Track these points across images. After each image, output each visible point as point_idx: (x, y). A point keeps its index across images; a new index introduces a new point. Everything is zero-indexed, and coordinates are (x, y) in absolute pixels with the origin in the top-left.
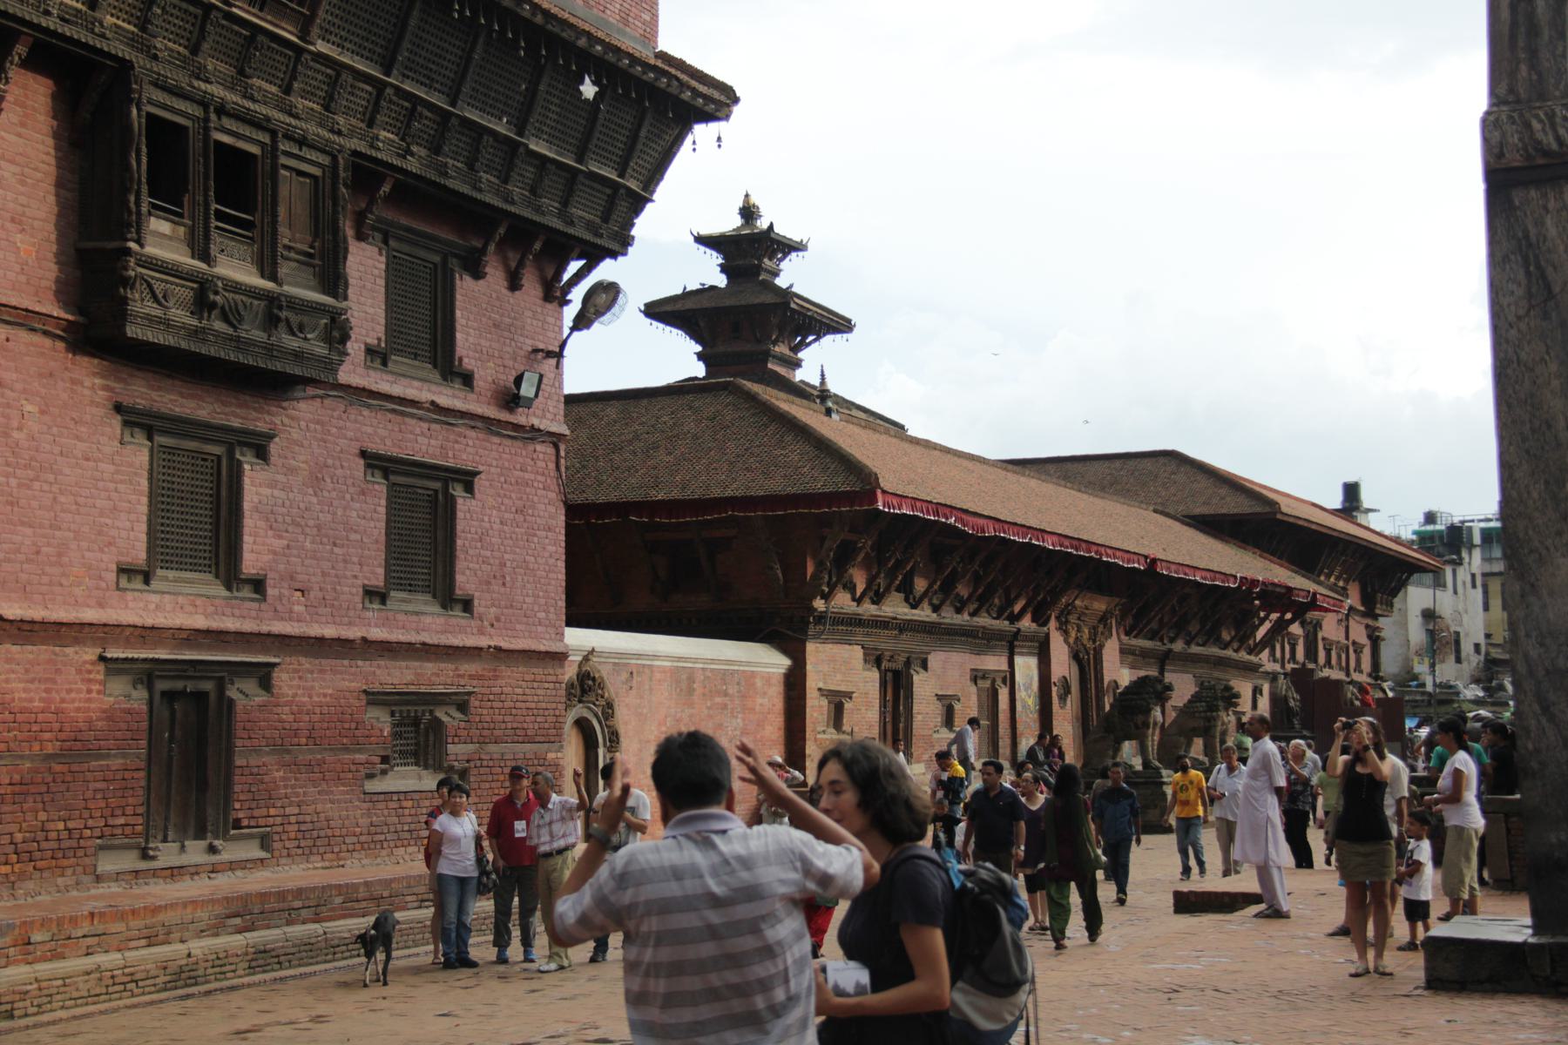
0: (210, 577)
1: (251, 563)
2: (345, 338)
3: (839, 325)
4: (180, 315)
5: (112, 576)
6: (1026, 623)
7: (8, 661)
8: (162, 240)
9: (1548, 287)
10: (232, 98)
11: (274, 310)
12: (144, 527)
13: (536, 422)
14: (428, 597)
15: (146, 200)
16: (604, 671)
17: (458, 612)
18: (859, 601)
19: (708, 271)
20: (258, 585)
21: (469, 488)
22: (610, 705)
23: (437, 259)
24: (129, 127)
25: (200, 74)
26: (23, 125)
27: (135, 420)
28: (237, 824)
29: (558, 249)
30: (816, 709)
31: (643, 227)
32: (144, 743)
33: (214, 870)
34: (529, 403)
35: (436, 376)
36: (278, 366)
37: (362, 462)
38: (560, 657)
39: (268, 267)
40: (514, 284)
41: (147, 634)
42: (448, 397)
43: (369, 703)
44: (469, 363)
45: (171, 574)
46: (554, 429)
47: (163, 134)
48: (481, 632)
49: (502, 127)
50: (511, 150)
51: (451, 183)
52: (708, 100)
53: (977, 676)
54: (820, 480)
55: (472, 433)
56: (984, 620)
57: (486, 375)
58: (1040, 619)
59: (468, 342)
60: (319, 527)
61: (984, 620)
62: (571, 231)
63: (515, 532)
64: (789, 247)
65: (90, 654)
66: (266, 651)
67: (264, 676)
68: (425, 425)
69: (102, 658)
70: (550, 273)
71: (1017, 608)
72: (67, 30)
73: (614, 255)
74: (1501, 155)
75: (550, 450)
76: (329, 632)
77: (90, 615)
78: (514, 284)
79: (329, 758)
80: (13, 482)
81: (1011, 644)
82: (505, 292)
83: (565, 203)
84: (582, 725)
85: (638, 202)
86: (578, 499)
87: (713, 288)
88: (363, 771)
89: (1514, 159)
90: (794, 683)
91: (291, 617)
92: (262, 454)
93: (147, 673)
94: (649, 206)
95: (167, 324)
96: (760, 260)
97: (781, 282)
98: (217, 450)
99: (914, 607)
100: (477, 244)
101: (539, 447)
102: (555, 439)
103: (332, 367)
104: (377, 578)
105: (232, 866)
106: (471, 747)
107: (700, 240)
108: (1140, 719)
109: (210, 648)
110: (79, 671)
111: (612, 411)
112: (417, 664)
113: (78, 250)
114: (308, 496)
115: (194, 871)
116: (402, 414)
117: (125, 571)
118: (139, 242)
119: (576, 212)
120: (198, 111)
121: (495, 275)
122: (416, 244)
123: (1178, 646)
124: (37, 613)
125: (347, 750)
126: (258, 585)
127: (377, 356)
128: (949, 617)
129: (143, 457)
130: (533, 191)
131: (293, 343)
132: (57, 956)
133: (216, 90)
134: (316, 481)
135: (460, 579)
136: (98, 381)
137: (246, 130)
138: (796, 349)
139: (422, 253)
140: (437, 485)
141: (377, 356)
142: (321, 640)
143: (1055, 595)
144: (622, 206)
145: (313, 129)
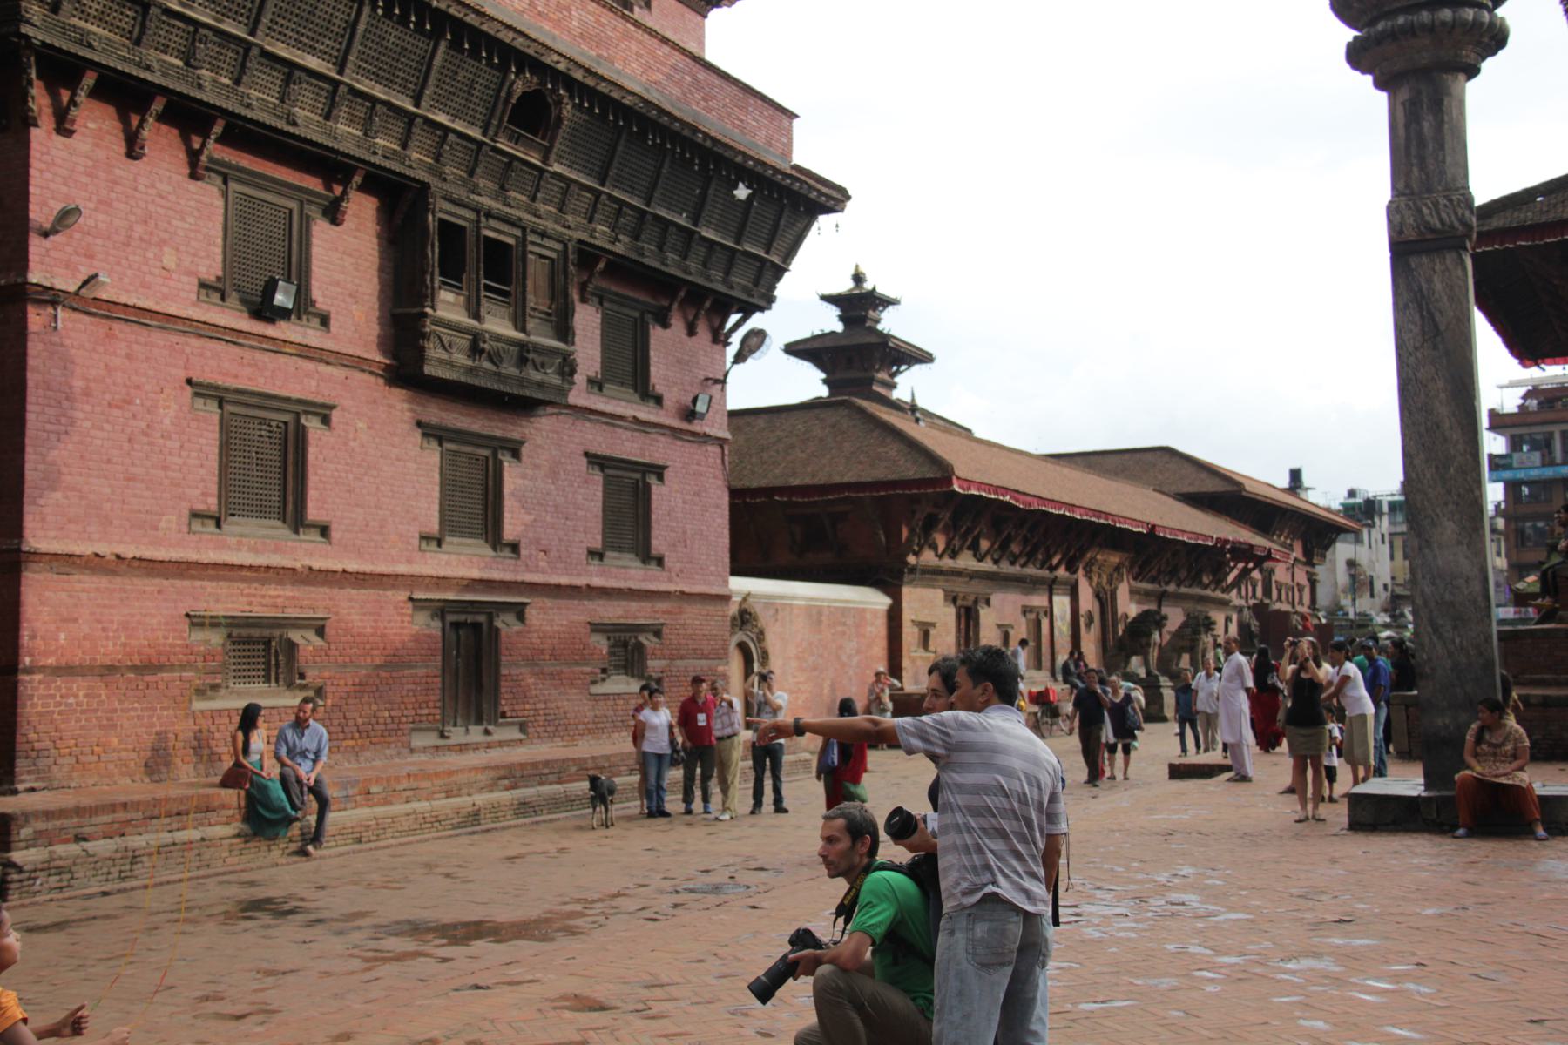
0: (482, 542)
1: (510, 531)
2: (573, 372)
3: (924, 358)
4: (461, 358)
5: (416, 542)
6: (1062, 572)
7: (350, 600)
8: (448, 305)
9: (1436, 326)
10: (496, 206)
11: (524, 354)
12: (437, 507)
13: (707, 430)
14: (632, 556)
15: (438, 278)
16: (757, 609)
17: (653, 566)
18: (940, 557)
19: (830, 321)
20: (515, 548)
21: (660, 478)
22: (762, 633)
23: (636, 314)
24: (426, 228)
25: (474, 190)
26: (358, 230)
27: (431, 432)
28: (503, 715)
29: (723, 306)
30: (910, 634)
31: (783, 289)
32: (439, 658)
33: (489, 746)
34: (702, 416)
35: (636, 398)
36: (527, 393)
37: (585, 460)
38: (725, 598)
39: (520, 323)
40: (691, 331)
41: (440, 582)
42: (646, 413)
43: (593, 631)
44: (660, 389)
45: (455, 540)
47: (450, 232)
48: (670, 580)
49: (682, 220)
50: (689, 235)
51: (646, 261)
52: (830, 198)
53: (1026, 611)
54: (910, 470)
55: (662, 439)
56: (1031, 570)
57: (674, 397)
58: (1071, 568)
59: (659, 373)
60: (556, 506)
61: (1031, 570)
62: (731, 293)
63: (694, 510)
64: (887, 302)
65: (402, 596)
66: (521, 594)
67: (519, 611)
68: (629, 433)
69: (411, 599)
70: (717, 323)
71: (1055, 561)
72: (387, 164)
73: (762, 309)
74: (1401, 232)
75: (718, 450)
76: (564, 580)
77: (402, 569)
78: (691, 331)
79: (565, 669)
80: (351, 476)
81: (1051, 587)
82: (685, 337)
83: (727, 273)
84: (743, 647)
85: (779, 272)
86: (738, 484)
87: (833, 333)
88: (589, 678)
89: (1411, 235)
90: (894, 617)
91: (537, 570)
92: (516, 454)
93: (441, 610)
94: (787, 274)
95: (451, 364)
96: (867, 311)
97: (880, 327)
98: (486, 452)
99: (980, 560)
100: (666, 303)
101: (710, 448)
102: (721, 442)
103: (564, 392)
104: (597, 542)
105: (501, 744)
106: (664, 662)
107: (825, 298)
108: (1144, 641)
109: (483, 592)
110: (396, 608)
111: (761, 422)
112: (624, 603)
113: (394, 316)
114: (549, 485)
115: (476, 747)
116: (613, 425)
117: (425, 538)
118: (433, 307)
119: (735, 279)
120: (472, 215)
121: (678, 325)
122: (622, 305)
123: (1171, 588)
124: (368, 568)
125: (577, 664)
126: (515, 548)
127: (595, 384)
128: (1006, 568)
130: (705, 265)
131: (537, 376)
132: (386, 802)
133: (486, 201)
134: (553, 474)
135: (654, 542)
136: (406, 406)
137: (505, 228)
138: (893, 375)
139: (626, 311)
140: (638, 476)
141: (595, 384)
142: (558, 587)
143: (1082, 552)
144: (768, 274)
145: (551, 226)
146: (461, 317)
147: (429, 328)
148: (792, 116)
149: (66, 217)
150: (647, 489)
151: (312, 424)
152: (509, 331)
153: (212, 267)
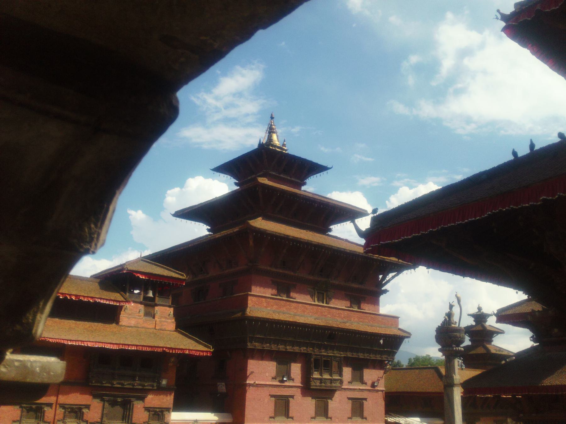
1: (330, 415)
2: (342, 383)
4: (318, 384)
8: (316, 375)
10: (325, 354)
11: (331, 381)
13: (379, 389)
20: (331, 418)
39: (331, 376)
46: (381, 389)
47: (317, 362)
95: (316, 386)
102: (382, 391)
117: (312, 418)
127: (350, 383)
129: (314, 402)
131: (334, 385)
141: (350, 383)
146: (319, 377)
147: (312, 380)
148: (398, 318)
149: (252, 372)
150: (363, 403)
151: (291, 399)
152: (329, 377)
153: (274, 374)
